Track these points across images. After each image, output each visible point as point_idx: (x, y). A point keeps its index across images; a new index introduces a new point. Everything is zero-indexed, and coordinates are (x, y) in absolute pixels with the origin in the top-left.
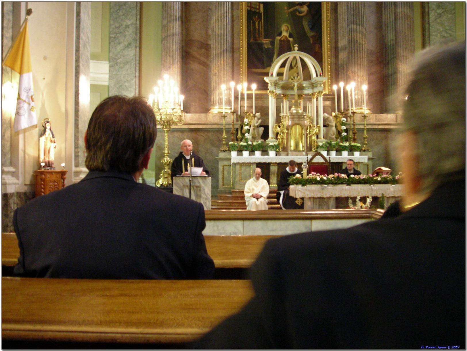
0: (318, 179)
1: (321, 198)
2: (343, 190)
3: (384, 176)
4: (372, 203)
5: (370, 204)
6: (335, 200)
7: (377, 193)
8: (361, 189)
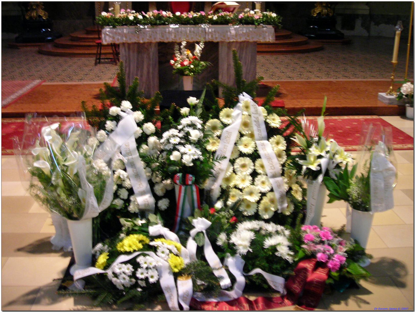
0: (131, 18)
1: (138, 44)
2: (166, 32)
3: (222, 14)
4: (204, 51)
5: (201, 52)
6: (157, 46)
7: (212, 36)
8: (190, 31)
